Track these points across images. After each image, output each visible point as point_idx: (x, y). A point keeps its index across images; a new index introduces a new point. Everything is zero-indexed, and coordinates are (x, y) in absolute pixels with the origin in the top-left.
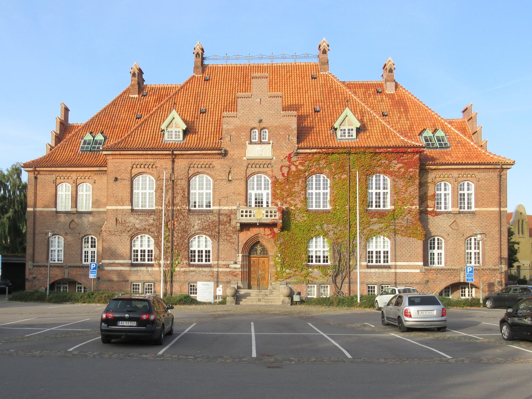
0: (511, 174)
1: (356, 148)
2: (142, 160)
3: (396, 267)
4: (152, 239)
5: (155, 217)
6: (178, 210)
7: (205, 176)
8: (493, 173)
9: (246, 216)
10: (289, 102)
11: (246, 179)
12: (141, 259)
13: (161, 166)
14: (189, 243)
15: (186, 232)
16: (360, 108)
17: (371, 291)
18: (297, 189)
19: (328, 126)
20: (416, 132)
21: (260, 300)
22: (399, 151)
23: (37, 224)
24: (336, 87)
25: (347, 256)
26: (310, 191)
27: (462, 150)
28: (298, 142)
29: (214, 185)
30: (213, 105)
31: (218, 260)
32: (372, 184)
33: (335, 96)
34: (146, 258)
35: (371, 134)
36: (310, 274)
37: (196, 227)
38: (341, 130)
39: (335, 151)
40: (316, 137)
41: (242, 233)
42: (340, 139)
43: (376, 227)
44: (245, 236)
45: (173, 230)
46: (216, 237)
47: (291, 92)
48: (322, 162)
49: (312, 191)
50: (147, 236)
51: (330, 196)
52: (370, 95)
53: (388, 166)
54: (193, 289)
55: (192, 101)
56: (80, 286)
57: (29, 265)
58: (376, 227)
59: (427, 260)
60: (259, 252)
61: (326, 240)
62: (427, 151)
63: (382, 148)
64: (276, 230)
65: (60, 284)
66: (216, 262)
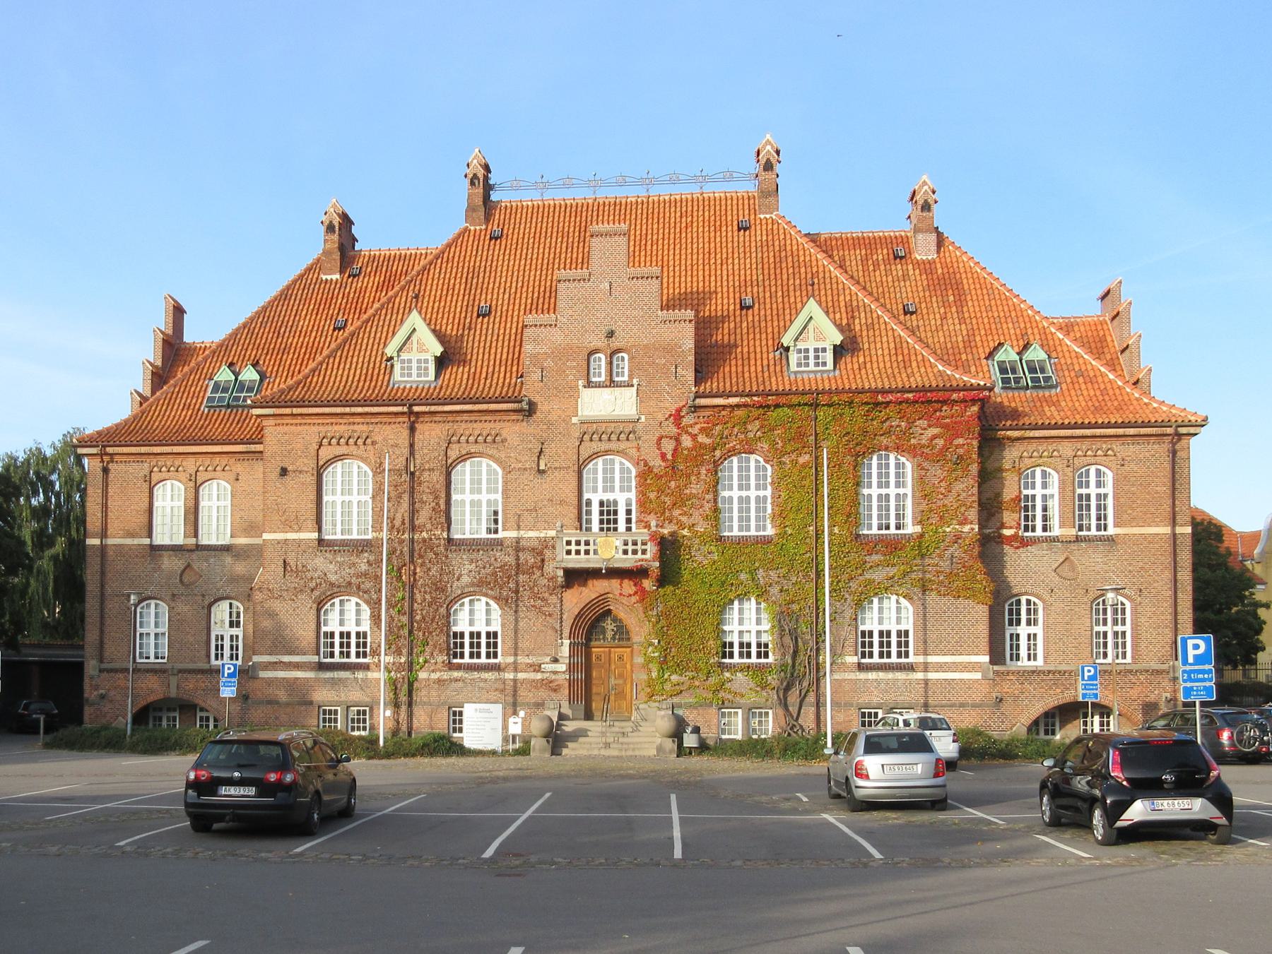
0: (1199, 449)
1: (830, 392)
2: (343, 428)
3: (926, 667)
4: (364, 607)
5: (372, 558)
6: (424, 540)
7: (485, 461)
8: (1156, 447)
9: (578, 552)
10: (683, 285)
11: (579, 467)
12: (342, 653)
13: (384, 439)
14: (449, 615)
15: (443, 590)
16: (848, 298)
18: (695, 488)
19: (770, 342)
20: (981, 350)
21: (607, 745)
22: (930, 399)
23: (109, 575)
24: (795, 248)
25: (812, 644)
26: (725, 494)
27: (1085, 393)
28: (697, 382)
29: (505, 483)
30: (507, 296)
31: (516, 655)
32: (870, 475)
33: (791, 271)
34: (353, 650)
35: (868, 359)
36: (728, 685)
37: (466, 579)
38: (799, 351)
39: (783, 400)
40: (740, 369)
41: (569, 591)
42: (796, 373)
43: (878, 575)
44: (576, 599)
45: (412, 587)
46: (510, 601)
47: (689, 262)
48: (754, 427)
49: (731, 494)
50: (354, 600)
51: (772, 504)
52: (876, 265)
53: (907, 434)
54: (457, 719)
55: (460, 287)
56: (204, 714)
57: (91, 667)
58: (878, 575)
59: (998, 650)
60: (609, 634)
61: (763, 605)
62: (1000, 395)
63: (890, 391)
64: (648, 584)
65: (161, 710)
66: (511, 659)
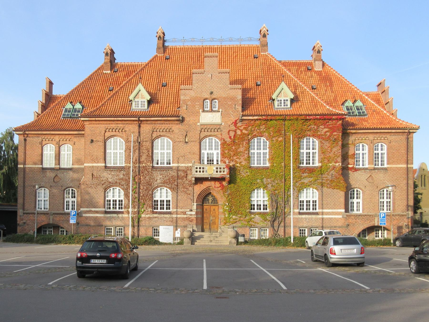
0: (416, 137)
1: (290, 115)
3: (323, 213)
4: (122, 191)
5: (125, 173)
6: (144, 167)
7: (166, 138)
8: (402, 136)
9: (200, 172)
10: (235, 77)
11: (200, 141)
12: (113, 207)
13: (129, 130)
14: (153, 194)
15: (151, 185)
16: (294, 82)
17: (303, 233)
18: (242, 149)
19: (267, 98)
20: (339, 102)
21: (211, 241)
22: (325, 118)
23: (27, 179)
24: (274, 65)
25: (283, 205)
26: (252, 151)
27: (376, 117)
28: (243, 111)
29: (173, 146)
30: (172, 80)
31: (177, 208)
32: (303, 145)
33: (273, 72)
34: (118, 206)
35: (302, 104)
36: (253, 220)
37: (159, 181)
38: (278, 101)
39: (273, 118)
40: (257, 107)
41: (196, 186)
42: (277, 108)
43: (306, 181)
44: (199, 188)
45: (139, 184)
46: (175, 189)
47: (237, 69)
48: (263, 127)
49: (254, 151)
50: (118, 188)
51: (269, 155)
52: (301, 72)
53: (316, 130)
54: (156, 232)
55: (155, 76)
56: (62, 230)
57: (20, 212)
58: (306, 181)
59: (347, 207)
60: (210, 201)
61: (265, 191)
62: (348, 118)
63: (311, 115)
64: (225, 183)
65: (46, 228)
66: (175, 210)
